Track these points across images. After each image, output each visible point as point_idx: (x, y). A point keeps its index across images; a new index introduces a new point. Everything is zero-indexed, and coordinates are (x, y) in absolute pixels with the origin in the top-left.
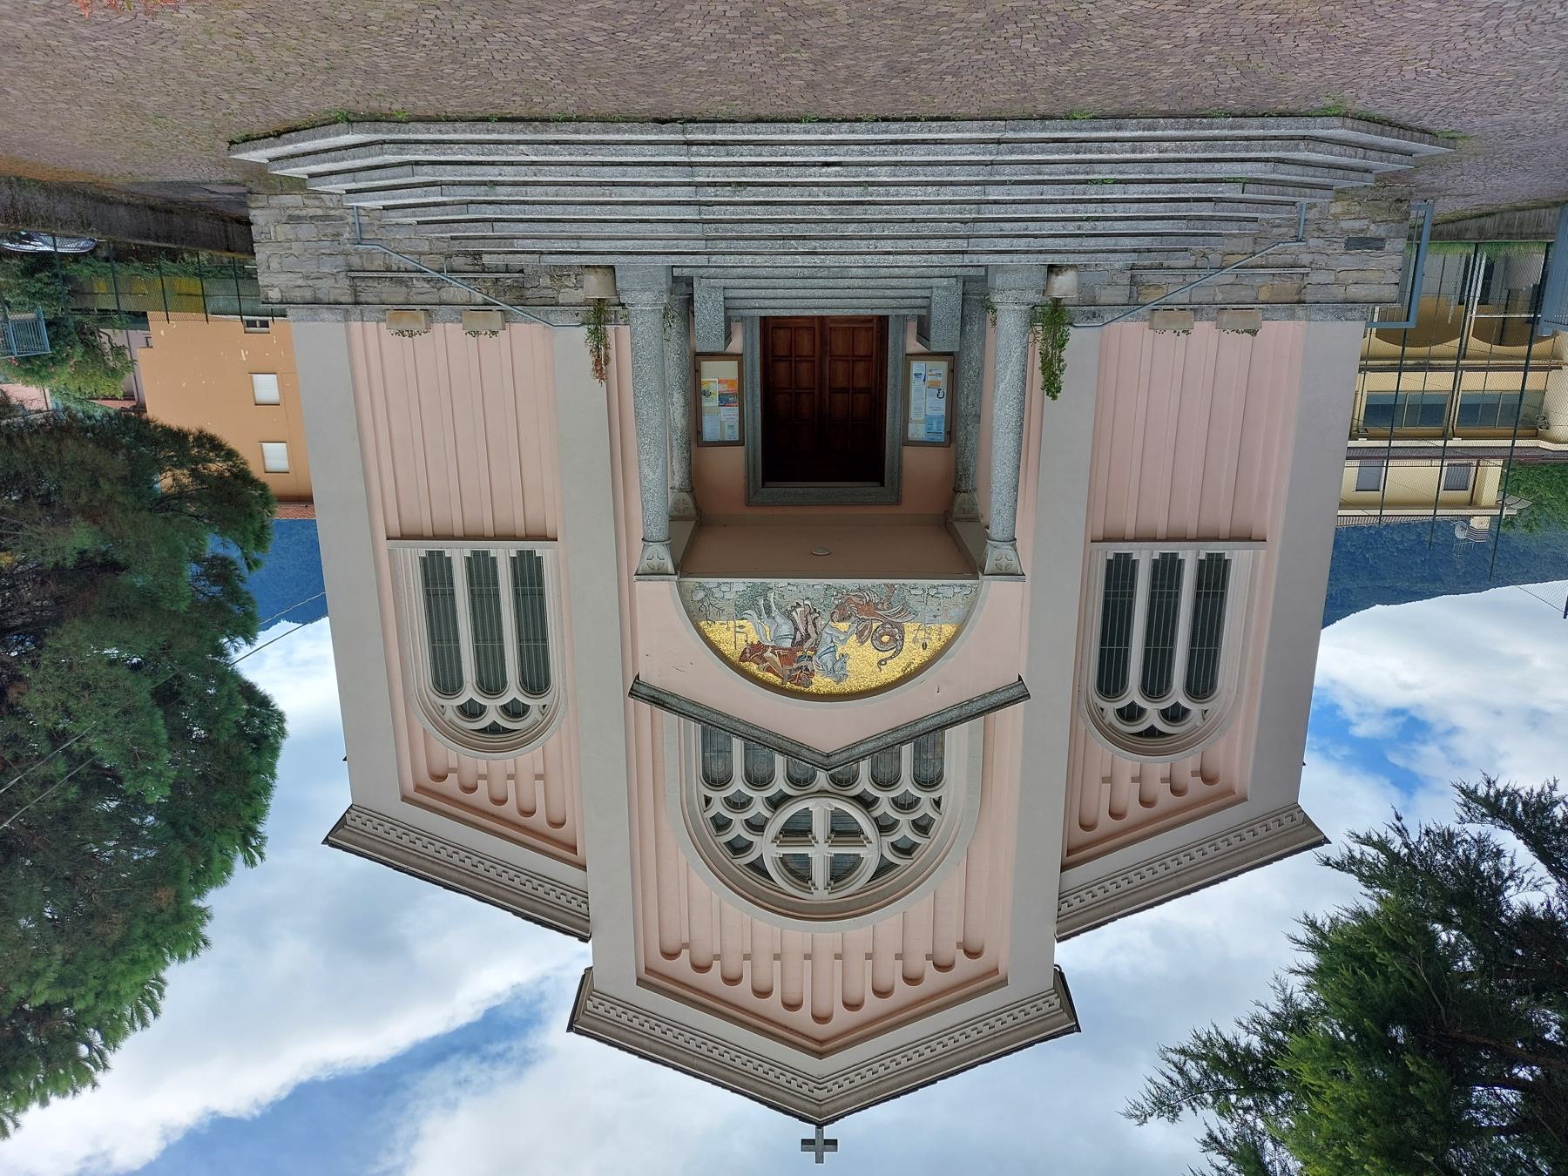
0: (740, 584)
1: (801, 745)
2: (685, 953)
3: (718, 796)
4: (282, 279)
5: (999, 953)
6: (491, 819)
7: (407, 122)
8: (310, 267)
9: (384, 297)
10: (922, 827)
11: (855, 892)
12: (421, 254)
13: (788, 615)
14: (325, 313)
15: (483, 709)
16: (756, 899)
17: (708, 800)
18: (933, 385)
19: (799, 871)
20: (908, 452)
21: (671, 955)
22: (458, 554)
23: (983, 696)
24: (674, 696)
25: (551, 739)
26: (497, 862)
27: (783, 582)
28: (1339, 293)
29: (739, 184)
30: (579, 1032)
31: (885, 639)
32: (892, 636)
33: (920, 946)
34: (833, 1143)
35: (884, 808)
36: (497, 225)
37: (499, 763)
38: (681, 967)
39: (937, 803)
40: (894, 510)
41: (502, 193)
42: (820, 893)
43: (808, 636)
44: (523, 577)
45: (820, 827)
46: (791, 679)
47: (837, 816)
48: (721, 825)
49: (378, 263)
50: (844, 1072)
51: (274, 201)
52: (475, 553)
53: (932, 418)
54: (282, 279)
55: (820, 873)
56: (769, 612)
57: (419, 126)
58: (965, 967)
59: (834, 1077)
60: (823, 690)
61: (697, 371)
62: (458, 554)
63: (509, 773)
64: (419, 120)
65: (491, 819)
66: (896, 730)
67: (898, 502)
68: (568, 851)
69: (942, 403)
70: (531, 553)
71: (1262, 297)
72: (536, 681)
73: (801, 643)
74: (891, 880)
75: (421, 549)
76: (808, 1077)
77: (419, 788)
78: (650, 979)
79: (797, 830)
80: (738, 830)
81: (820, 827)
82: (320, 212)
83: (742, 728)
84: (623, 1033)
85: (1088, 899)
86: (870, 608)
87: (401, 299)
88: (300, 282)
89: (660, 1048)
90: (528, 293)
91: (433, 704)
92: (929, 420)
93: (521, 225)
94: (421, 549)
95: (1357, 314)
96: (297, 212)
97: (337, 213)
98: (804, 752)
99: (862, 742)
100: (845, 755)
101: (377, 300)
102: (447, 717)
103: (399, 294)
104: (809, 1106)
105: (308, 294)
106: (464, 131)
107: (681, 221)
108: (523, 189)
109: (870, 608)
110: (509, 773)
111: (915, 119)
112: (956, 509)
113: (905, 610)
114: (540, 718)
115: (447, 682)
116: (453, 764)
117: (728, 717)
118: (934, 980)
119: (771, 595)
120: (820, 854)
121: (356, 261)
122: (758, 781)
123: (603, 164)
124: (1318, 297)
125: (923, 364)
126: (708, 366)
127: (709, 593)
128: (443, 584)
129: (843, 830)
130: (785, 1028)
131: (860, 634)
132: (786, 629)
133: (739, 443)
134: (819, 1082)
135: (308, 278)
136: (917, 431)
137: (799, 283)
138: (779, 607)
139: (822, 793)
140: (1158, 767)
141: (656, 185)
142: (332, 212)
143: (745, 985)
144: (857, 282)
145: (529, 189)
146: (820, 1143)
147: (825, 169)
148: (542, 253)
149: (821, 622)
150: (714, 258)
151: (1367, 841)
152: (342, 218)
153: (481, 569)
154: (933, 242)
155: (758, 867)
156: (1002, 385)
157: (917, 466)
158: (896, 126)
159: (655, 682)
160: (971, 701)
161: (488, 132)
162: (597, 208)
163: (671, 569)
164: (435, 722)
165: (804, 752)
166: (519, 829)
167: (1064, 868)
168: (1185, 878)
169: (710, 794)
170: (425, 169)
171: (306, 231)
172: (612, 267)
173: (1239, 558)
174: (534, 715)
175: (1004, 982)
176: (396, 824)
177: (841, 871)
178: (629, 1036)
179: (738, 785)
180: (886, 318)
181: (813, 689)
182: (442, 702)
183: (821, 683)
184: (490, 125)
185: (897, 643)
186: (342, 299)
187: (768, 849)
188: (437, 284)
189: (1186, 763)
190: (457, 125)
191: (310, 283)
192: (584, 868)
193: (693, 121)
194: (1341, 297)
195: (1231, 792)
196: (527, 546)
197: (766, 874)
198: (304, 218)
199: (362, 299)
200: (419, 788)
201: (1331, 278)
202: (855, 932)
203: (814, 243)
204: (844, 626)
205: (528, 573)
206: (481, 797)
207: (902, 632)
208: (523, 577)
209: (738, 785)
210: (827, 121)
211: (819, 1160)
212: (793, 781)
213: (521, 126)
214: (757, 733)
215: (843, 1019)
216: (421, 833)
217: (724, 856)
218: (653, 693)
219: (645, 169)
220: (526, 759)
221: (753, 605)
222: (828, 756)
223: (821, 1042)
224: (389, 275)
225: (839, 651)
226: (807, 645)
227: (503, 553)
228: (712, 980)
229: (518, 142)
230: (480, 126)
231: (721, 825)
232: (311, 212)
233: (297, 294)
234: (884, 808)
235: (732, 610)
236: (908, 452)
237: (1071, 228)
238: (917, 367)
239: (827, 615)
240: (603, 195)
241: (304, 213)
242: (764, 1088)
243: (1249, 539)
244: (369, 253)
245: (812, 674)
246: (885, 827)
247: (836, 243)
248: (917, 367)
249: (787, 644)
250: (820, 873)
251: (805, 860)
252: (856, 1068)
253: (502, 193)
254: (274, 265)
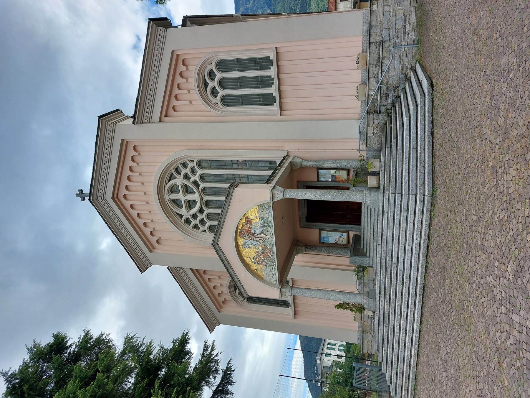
0: (271, 219)
1: (219, 236)
2: (136, 154)
3: (194, 164)
4: (380, 12)
5: (159, 249)
6: (171, 85)
7: (430, 215)
8: (385, 25)
9: (372, 54)
10: (196, 227)
11: (170, 208)
12: (388, 72)
13: (262, 232)
14: (367, 27)
15: (213, 79)
16: (161, 178)
17: (193, 161)
18: (339, 240)
19: (173, 190)
20: (317, 231)
21: (135, 148)
22: (272, 72)
23: (243, 287)
24: (231, 199)
25: (204, 106)
26: (155, 88)
27: (273, 231)
28: (365, 341)
29: (403, 283)
30: (99, 121)
31: (258, 260)
32: (259, 261)
33: (157, 227)
34: (84, 199)
35: (200, 217)
36: (393, 195)
37: (192, 84)
38: (131, 153)
39: (205, 231)
40: (298, 226)
41: (404, 214)
42: (168, 197)
43: (256, 238)
44: (265, 98)
45: (190, 197)
46: (241, 232)
47: (195, 202)
48: (185, 165)
49: (385, 54)
50: (109, 206)
51: (413, 10)
52: (273, 79)
53: (328, 239)
54: (380, 12)
55: (174, 196)
56: (262, 226)
57: (429, 218)
58: (153, 240)
59: (106, 202)
60: (239, 241)
61: (343, 169)
62: (272, 72)
63: (190, 95)
64: (431, 218)
65: (171, 85)
66: (229, 263)
67: (301, 227)
68: (165, 114)
69: (333, 242)
70: (273, 83)
71: (364, 323)
72: (226, 101)
73: (253, 235)
74: (177, 218)
75: (273, 58)
76: (104, 194)
77: (178, 55)
78: (124, 144)
79: (187, 190)
80: (184, 171)
81: (190, 197)
82: (407, 30)
83: (223, 219)
84: (103, 136)
85: (182, 275)
86: (267, 256)
87: (371, 62)
88: (379, 20)
89: (101, 148)
90: (372, 115)
91: (213, 60)
92: (328, 238)
93: (393, 203)
94: (273, 58)
95: (359, 342)
96: (408, 20)
97: (406, 38)
98: (217, 237)
99: (223, 253)
100: (218, 249)
101: (371, 51)
102: (208, 65)
103: (373, 61)
104: (95, 196)
105: (374, 23)
106: (425, 232)
107: (392, 251)
108: (405, 220)
109: (267, 256)
110: (190, 95)
111: (418, 351)
112: (300, 248)
113: (268, 266)
114: (213, 102)
115: (222, 65)
116: (190, 68)
117: (226, 215)
118: (147, 231)
119: (268, 228)
120: (180, 196)
121: (386, 45)
122: (202, 177)
123: (412, 253)
124: (364, 336)
125: (346, 236)
126: (345, 172)
127: (268, 209)
128: (260, 66)
129: (190, 204)
130: (119, 186)
131: (258, 252)
132: (258, 231)
133: (318, 181)
134: (104, 198)
135: (381, 23)
136: (324, 234)
137: (372, 223)
138: (265, 230)
139: (202, 199)
140: (226, 290)
141: (404, 260)
142: (407, 36)
143: (130, 174)
144: (372, 244)
145: (405, 222)
146: (83, 195)
147: (406, 313)
148: (384, 193)
149: (261, 241)
150: (380, 246)
151: (213, 345)
152: (404, 39)
153: (267, 82)
154: (383, 311)
155: (171, 177)
156: (339, 296)
157: (312, 234)
158: (417, 347)
159: (234, 193)
160: (241, 283)
161: (425, 240)
162: (398, 234)
163: (275, 200)
164: (205, 62)
165: (217, 237)
166: (170, 95)
167: (192, 270)
168: (194, 299)
169: (195, 162)
170: (414, 199)
171: (400, 24)
172: (379, 188)
173: (290, 311)
174: (214, 100)
175: (151, 251)
176: (162, 48)
177: (176, 202)
178: (102, 138)
179: (200, 172)
180: (360, 225)
181: (239, 238)
182: (214, 64)
183: (241, 241)
184: (427, 240)
185: (257, 263)
186: (371, 38)
187: (179, 181)
188: (377, 77)
189: (228, 297)
190: (428, 230)
191: (379, 24)
192: (160, 121)
193: (423, 297)
194: (364, 341)
195: (221, 308)
196: (276, 81)
197: (170, 180)
198: (405, 23)
199: (372, 45)
200: (178, 55)
201: (369, 339)
202: (156, 207)
203: (384, 280)
204: (260, 248)
205: (267, 100)
206: (179, 80)
207: (260, 264)
208: (265, 98)
209: (200, 172)
210: (420, 331)
211: (77, 195)
212: (204, 189)
213: (426, 249)
214: (222, 224)
215: (127, 204)
216: (161, 58)
217: (174, 166)
218: (231, 193)
219: (409, 265)
220: (195, 95)
221: (265, 222)
222: (217, 244)
223: (117, 197)
224: (381, 59)
225: (252, 246)
226: (253, 237)
227: (273, 90)
228: (129, 163)
229: (421, 238)
230: (427, 237)
231: (185, 165)
232: (407, 26)
233: (374, 18)
234: (200, 217)
235: (262, 216)
236: (317, 231)
237: (385, 349)
238: (345, 234)
239: (263, 243)
240: (402, 244)
241: (407, 23)
242: (97, 182)
243: (295, 314)
244: (390, 50)
245: (243, 238)
246: (194, 216)
247: (383, 286)
248: (345, 234)
249: (253, 231)
250: (174, 196)
251: (178, 192)
252: (112, 209)
253: (404, 214)
254: (386, 8)
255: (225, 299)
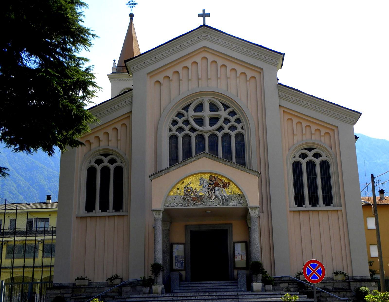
0: (231, 205)
3: (239, 130)
10: (175, 122)
13: (217, 197)
27: (218, 206)
30: (281, 53)
31: (189, 191)
32: (187, 191)
35: (187, 128)
39: (170, 130)
43: (211, 190)
45: (207, 121)
46: (215, 178)
48: (238, 121)
68: (285, 111)
79: (214, 120)
80: (233, 119)
81: (207, 121)
86: (194, 199)
109: (194, 199)
119: (221, 202)
120: (207, 113)
127: (239, 202)
131: (196, 192)
132: (217, 193)
138: (219, 199)
139: (207, 132)
149: (207, 195)
155: (226, 107)
163: (250, 209)
169: (242, 131)
181: (209, 175)
187: (223, 114)
204: (201, 194)
207: (184, 193)
212: (216, 136)
221: (227, 199)
226: (211, 188)
234: (187, 128)
235: (233, 198)
239: (206, 197)
245: (209, 180)
246: (187, 122)
249: (217, 188)
251: (211, 110)
255: (93, 143)
